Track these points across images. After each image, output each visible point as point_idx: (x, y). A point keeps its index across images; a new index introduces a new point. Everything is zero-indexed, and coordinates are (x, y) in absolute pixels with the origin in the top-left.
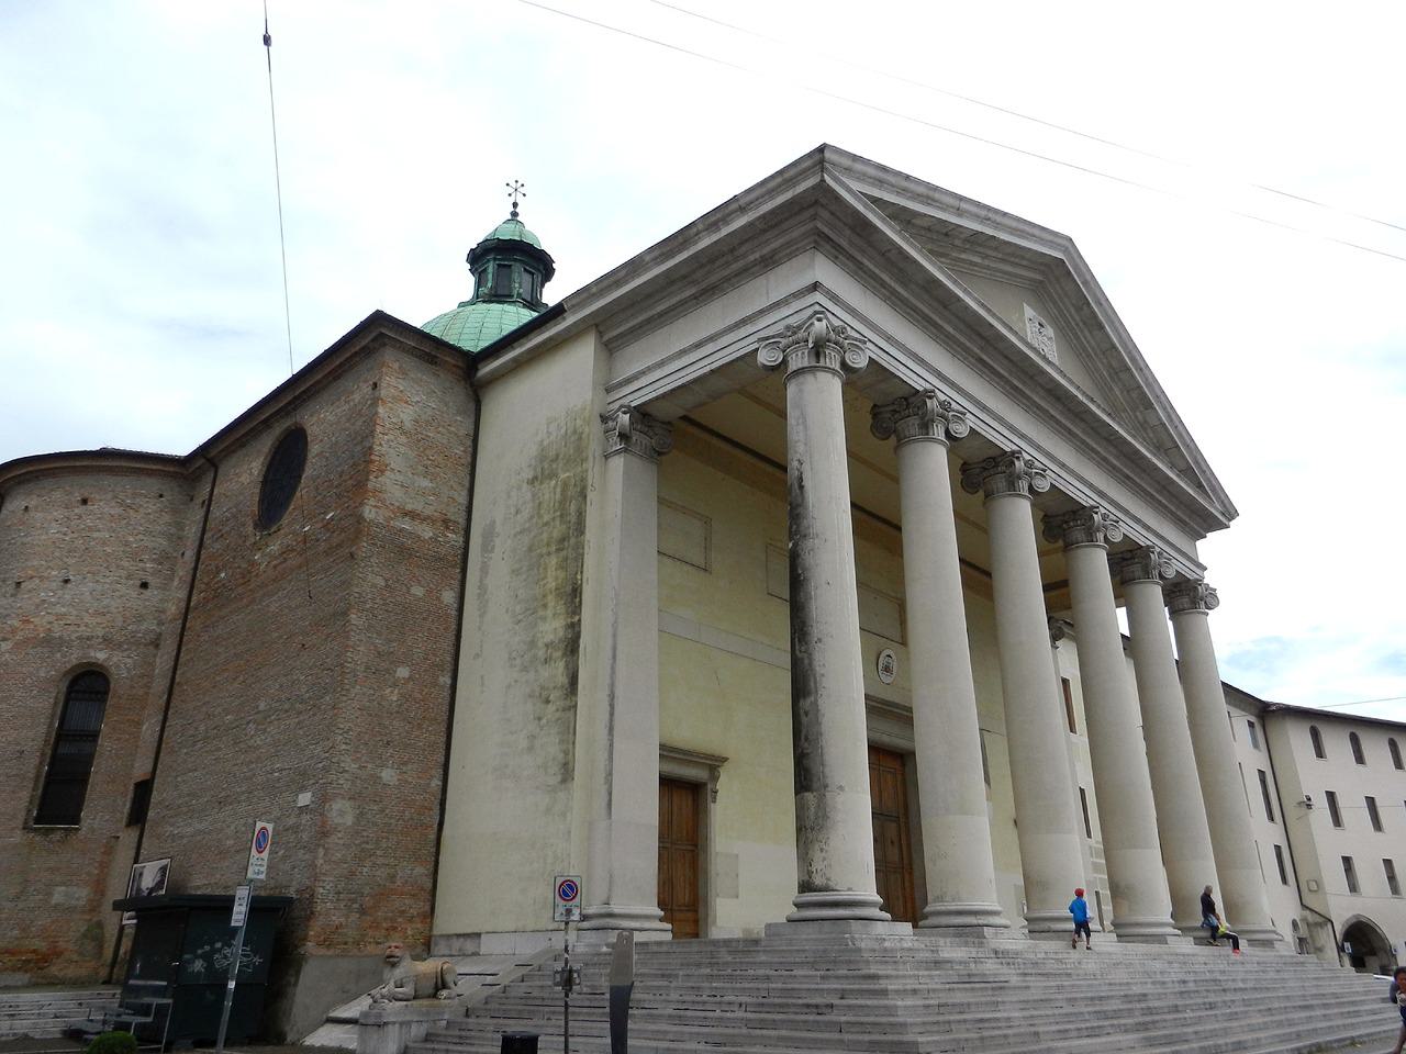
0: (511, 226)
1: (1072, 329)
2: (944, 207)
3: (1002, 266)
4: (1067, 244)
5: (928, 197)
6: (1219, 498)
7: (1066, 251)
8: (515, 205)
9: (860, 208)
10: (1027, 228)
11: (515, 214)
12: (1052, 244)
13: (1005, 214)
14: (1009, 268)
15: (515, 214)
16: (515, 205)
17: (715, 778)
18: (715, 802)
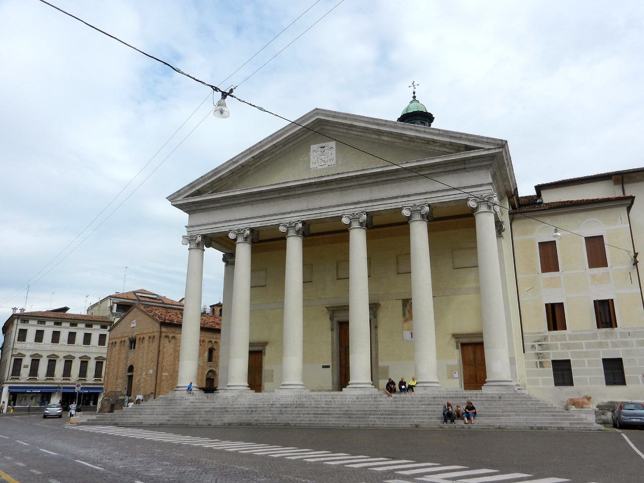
0: (414, 104)
1: (346, 133)
2: (228, 167)
3: (287, 147)
4: (317, 111)
5: (215, 173)
6: (482, 142)
7: (317, 114)
8: (414, 93)
9: (186, 202)
10: (279, 133)
11: (414, 97)
12: (310, 117)
13: (260, 142)
14: (290, 145)
15: (414, 97)
16: (414, 93)
17: (265, 349)
18: (264, 355)
